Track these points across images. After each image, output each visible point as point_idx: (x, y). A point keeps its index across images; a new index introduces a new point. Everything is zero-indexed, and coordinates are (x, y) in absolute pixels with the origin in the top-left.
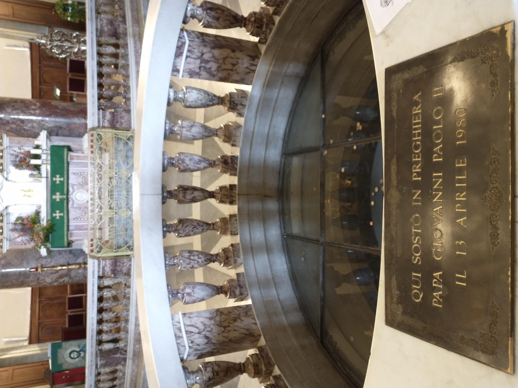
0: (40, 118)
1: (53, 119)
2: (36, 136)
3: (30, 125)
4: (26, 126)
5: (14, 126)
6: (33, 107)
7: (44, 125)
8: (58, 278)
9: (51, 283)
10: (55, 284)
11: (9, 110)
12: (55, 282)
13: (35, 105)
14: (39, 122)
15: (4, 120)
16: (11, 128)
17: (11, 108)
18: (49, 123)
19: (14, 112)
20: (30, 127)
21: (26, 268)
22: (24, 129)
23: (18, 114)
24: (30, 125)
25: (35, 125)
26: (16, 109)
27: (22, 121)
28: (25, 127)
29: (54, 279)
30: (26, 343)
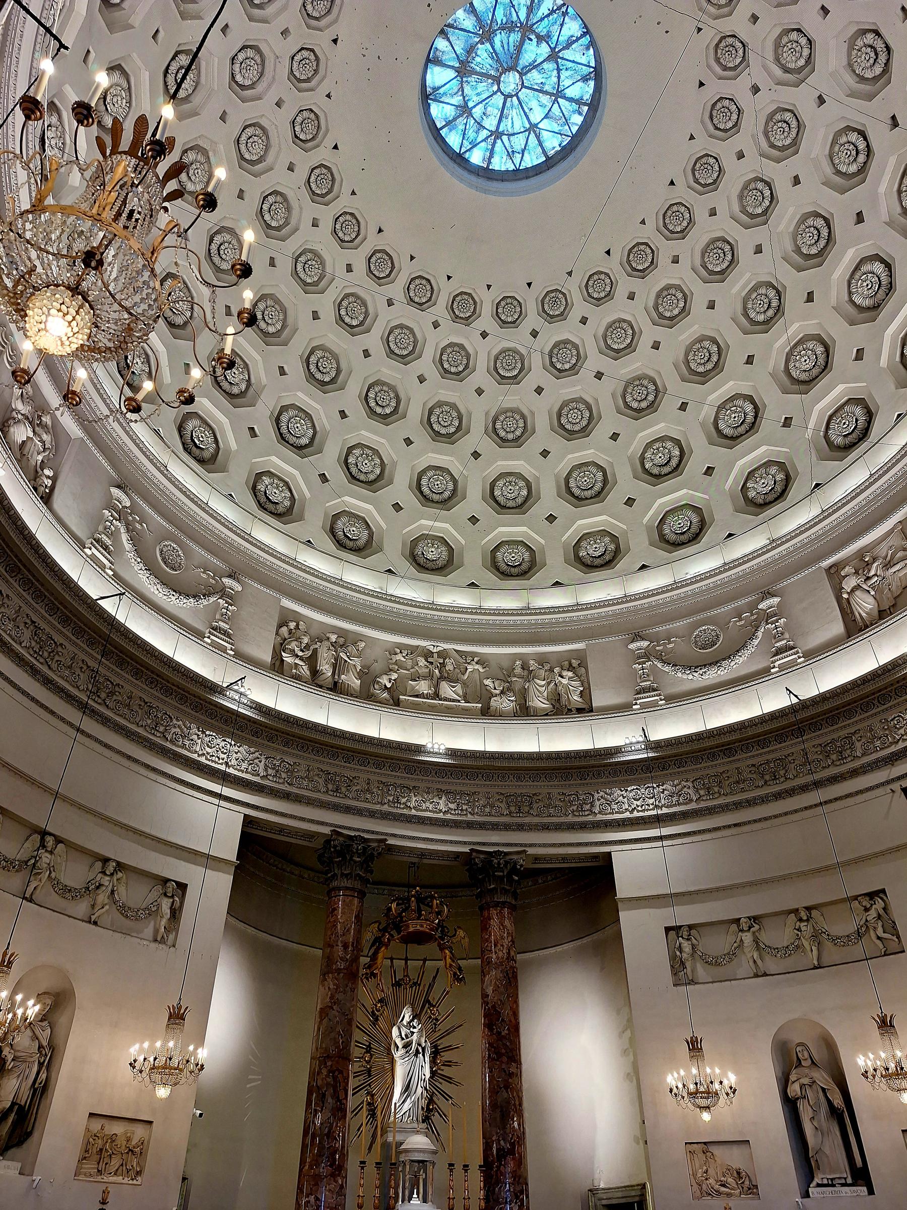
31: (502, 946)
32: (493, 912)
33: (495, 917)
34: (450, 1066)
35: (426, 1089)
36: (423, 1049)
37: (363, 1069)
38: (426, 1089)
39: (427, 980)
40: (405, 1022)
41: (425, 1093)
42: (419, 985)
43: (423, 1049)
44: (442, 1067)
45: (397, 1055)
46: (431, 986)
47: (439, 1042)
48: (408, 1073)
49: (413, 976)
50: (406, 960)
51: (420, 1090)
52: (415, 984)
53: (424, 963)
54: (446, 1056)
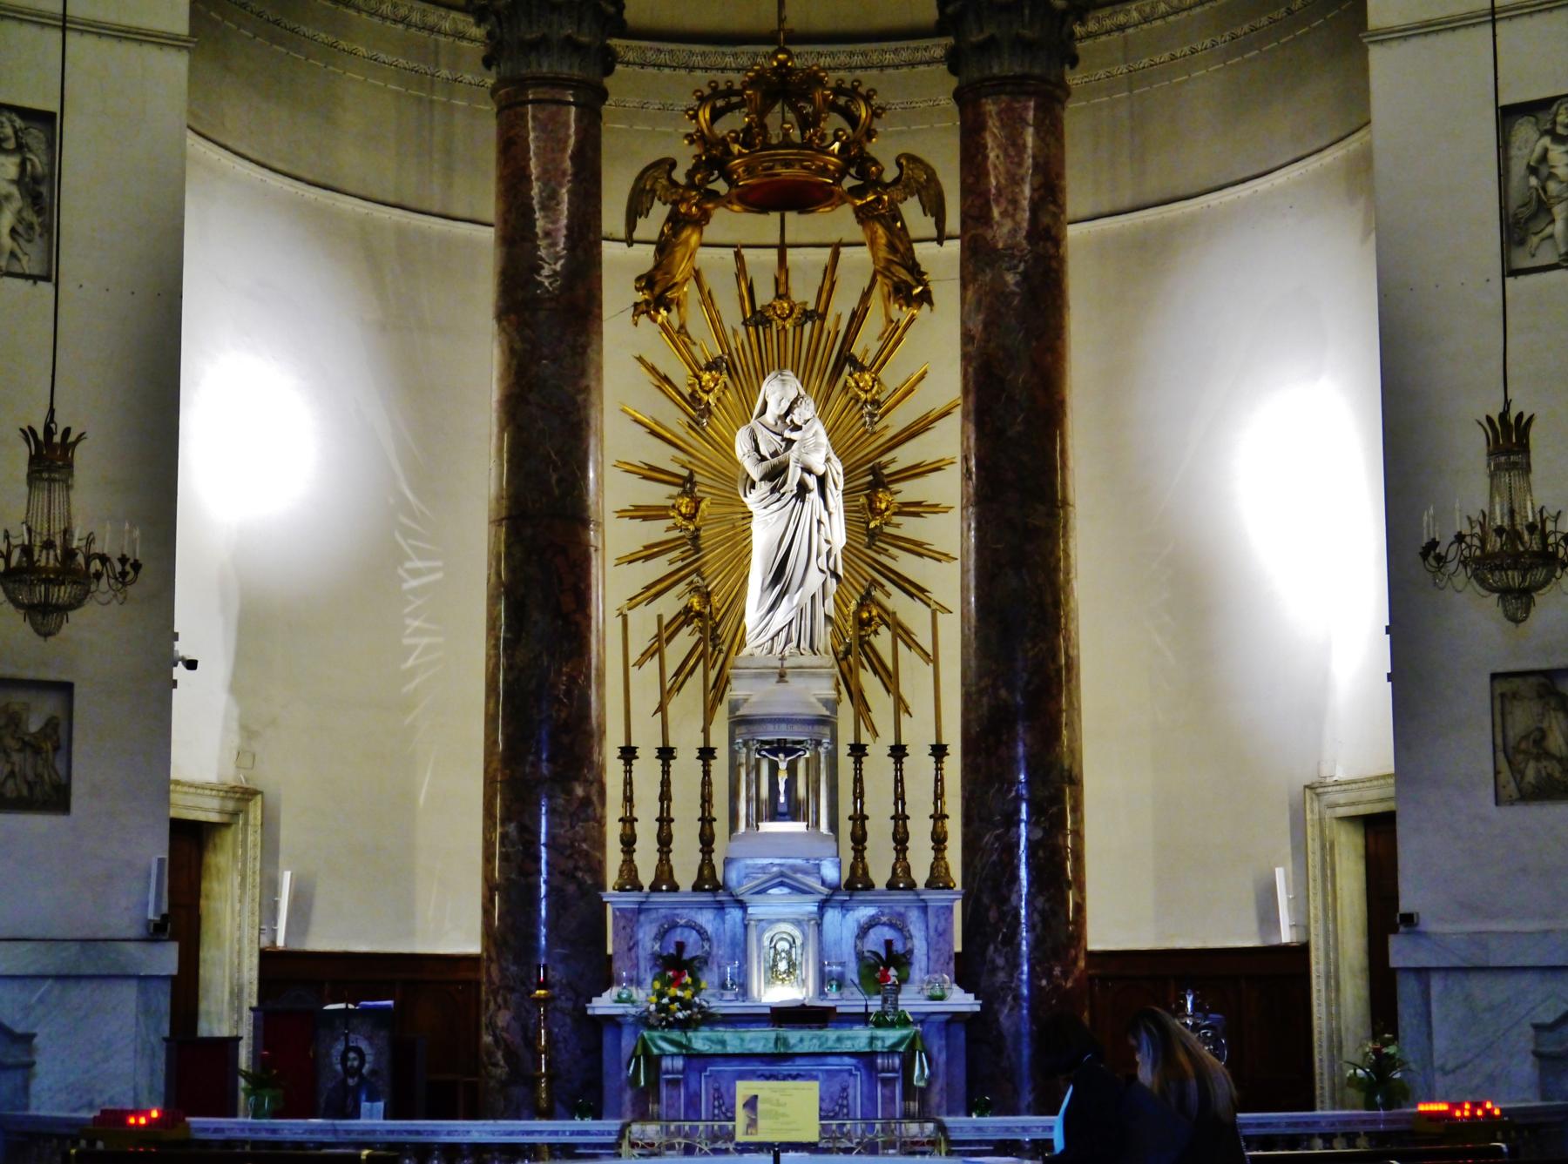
0: (1025, 991)
1: (1025, 1028)
2: (965, 981)
3: (1000, 962)
4: (996, 950)
5: (993, 915)
6: (1057, 971)
7: (1004, 1002)
8: (507, 1046)
9: (492, 1025)
10: (487, 1039)
11: (1040, 902)
12: (495, 1035)
13: (1065, 974)
14: (1011, 988)
15: (1010, 891)
16: (988, 909)
17: (1047, 906)
18: (1009, 1016)
19: (1036, 917)
20: (993, 961)
21: (548, 954)
22: (987, 944)
23: (1031, 928)
24: (1000, 962)
25: (1002, 976)
26: (1044, 920)
27: (1012, 939)
28: (992, 947)
29: (505, 1035)
30: (265, 942)
31: (1014, 202)
32: (990, 107)
33: (993, 124)
34: (917, 514)
35: (834, 574)
36: (822, 480)
37: (676, 534)
38: (834, 574)
39: (842, 305)
40: (769, 418)
41: (832, 585)
42: (823, 317)
43: (822, 480)
44: (896, 519)
45: (752, 500)
46: (857, 318)
47: (884, 459)
48: (793, 535)
49: (804, 293)
50: (782, 248)
51: (815, 579)
52: (808, 315)
53: (835, 256)
54: (909, 491)
